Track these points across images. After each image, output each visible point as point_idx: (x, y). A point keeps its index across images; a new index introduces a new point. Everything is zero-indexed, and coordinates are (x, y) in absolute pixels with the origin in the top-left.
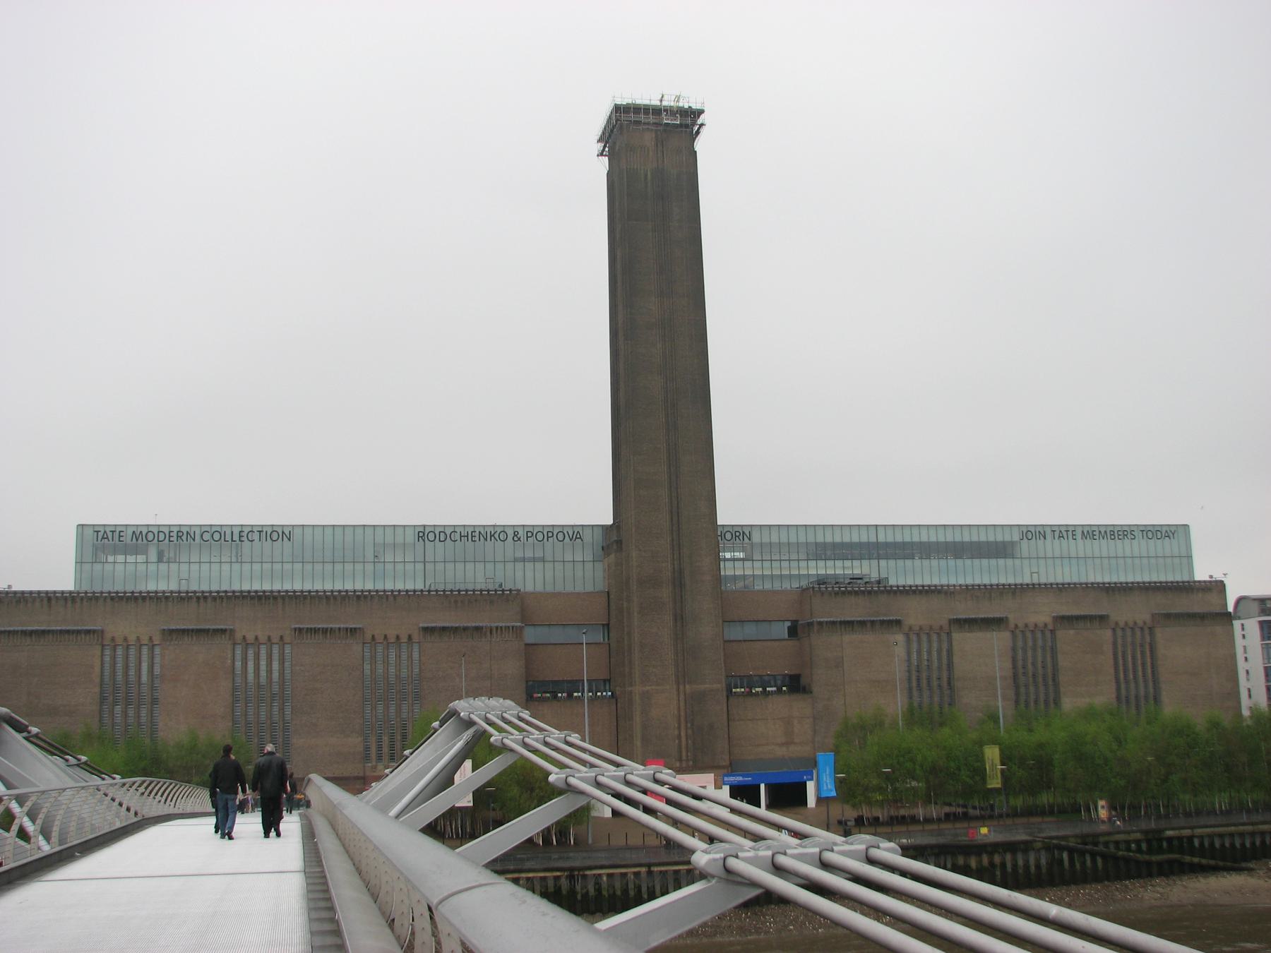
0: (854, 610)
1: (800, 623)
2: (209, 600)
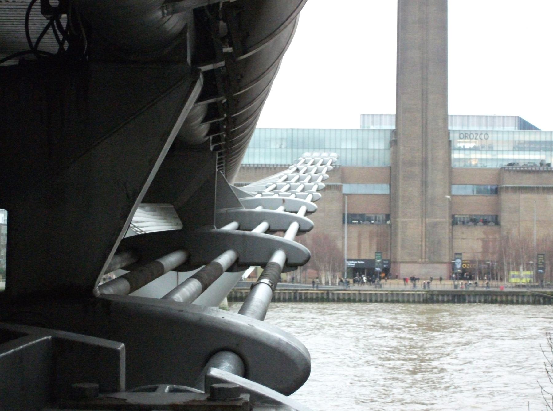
0: (528, 181)
1: (499, 186)
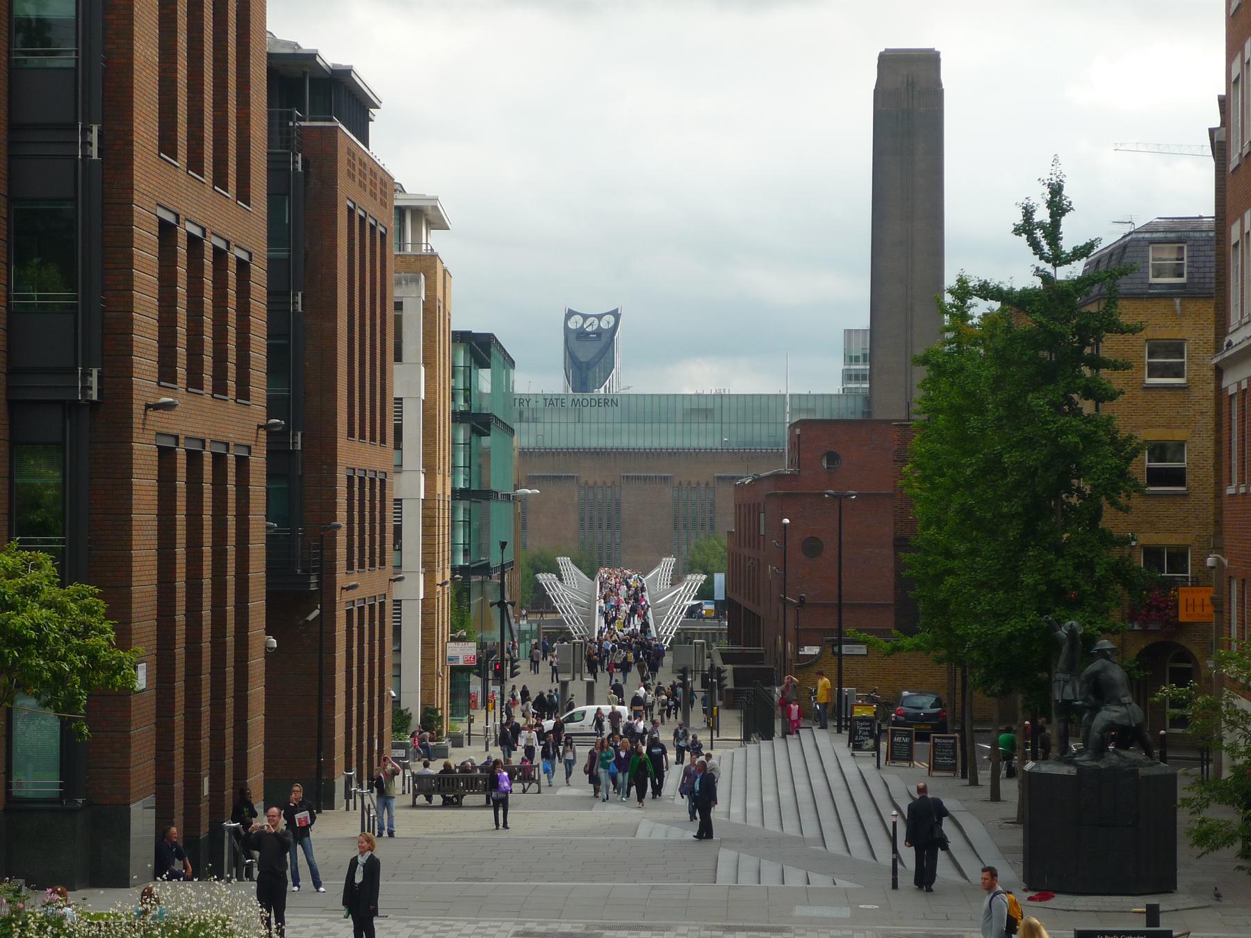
2: (561, 455)
